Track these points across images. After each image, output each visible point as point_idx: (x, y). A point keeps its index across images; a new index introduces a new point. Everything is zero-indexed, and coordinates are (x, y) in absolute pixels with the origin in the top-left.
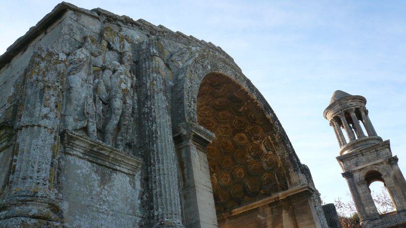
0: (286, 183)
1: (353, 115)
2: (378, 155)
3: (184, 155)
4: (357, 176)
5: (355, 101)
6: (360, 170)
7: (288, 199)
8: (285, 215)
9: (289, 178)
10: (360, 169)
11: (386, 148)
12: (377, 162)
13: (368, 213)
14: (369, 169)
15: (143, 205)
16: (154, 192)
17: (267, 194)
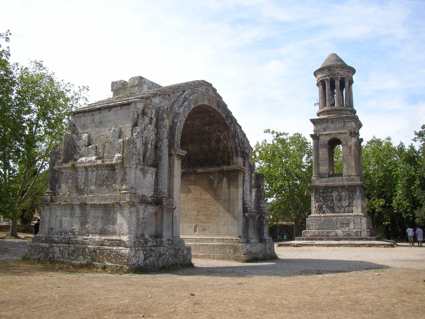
0: (230, 162)
1: (337, 83)
2: (344, 125)
3: (171, 162)
4: (322, 138)
5: (343, 70)
6: (326, 135)
7: (229, 172)
8: (225, 180)
9: (233, 159)
10: (326, 134)
11: (352, 121)
12: (342, 131)
13: (321, 172)
14: (333, 136)
15: (155, 184)
16: (159, 180)
17: (219, 165)
